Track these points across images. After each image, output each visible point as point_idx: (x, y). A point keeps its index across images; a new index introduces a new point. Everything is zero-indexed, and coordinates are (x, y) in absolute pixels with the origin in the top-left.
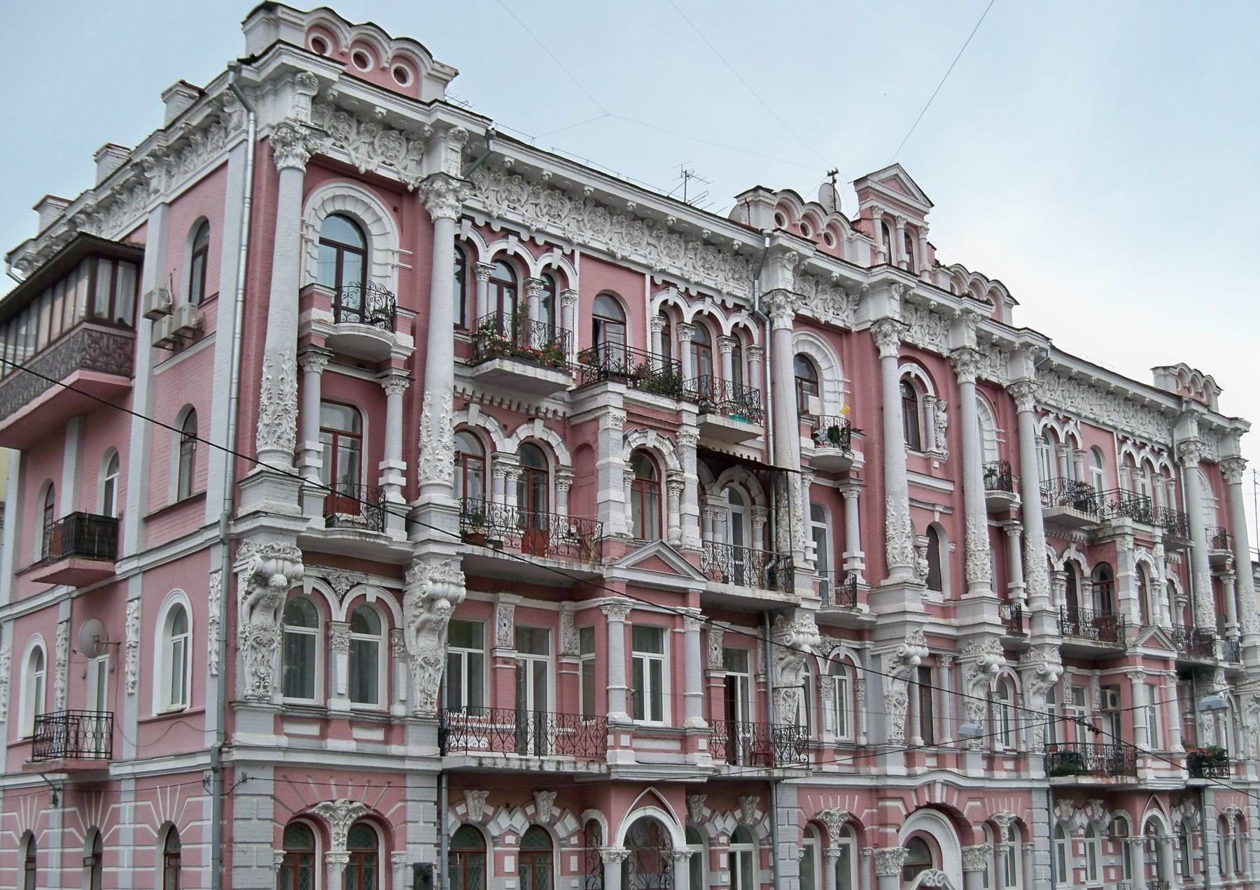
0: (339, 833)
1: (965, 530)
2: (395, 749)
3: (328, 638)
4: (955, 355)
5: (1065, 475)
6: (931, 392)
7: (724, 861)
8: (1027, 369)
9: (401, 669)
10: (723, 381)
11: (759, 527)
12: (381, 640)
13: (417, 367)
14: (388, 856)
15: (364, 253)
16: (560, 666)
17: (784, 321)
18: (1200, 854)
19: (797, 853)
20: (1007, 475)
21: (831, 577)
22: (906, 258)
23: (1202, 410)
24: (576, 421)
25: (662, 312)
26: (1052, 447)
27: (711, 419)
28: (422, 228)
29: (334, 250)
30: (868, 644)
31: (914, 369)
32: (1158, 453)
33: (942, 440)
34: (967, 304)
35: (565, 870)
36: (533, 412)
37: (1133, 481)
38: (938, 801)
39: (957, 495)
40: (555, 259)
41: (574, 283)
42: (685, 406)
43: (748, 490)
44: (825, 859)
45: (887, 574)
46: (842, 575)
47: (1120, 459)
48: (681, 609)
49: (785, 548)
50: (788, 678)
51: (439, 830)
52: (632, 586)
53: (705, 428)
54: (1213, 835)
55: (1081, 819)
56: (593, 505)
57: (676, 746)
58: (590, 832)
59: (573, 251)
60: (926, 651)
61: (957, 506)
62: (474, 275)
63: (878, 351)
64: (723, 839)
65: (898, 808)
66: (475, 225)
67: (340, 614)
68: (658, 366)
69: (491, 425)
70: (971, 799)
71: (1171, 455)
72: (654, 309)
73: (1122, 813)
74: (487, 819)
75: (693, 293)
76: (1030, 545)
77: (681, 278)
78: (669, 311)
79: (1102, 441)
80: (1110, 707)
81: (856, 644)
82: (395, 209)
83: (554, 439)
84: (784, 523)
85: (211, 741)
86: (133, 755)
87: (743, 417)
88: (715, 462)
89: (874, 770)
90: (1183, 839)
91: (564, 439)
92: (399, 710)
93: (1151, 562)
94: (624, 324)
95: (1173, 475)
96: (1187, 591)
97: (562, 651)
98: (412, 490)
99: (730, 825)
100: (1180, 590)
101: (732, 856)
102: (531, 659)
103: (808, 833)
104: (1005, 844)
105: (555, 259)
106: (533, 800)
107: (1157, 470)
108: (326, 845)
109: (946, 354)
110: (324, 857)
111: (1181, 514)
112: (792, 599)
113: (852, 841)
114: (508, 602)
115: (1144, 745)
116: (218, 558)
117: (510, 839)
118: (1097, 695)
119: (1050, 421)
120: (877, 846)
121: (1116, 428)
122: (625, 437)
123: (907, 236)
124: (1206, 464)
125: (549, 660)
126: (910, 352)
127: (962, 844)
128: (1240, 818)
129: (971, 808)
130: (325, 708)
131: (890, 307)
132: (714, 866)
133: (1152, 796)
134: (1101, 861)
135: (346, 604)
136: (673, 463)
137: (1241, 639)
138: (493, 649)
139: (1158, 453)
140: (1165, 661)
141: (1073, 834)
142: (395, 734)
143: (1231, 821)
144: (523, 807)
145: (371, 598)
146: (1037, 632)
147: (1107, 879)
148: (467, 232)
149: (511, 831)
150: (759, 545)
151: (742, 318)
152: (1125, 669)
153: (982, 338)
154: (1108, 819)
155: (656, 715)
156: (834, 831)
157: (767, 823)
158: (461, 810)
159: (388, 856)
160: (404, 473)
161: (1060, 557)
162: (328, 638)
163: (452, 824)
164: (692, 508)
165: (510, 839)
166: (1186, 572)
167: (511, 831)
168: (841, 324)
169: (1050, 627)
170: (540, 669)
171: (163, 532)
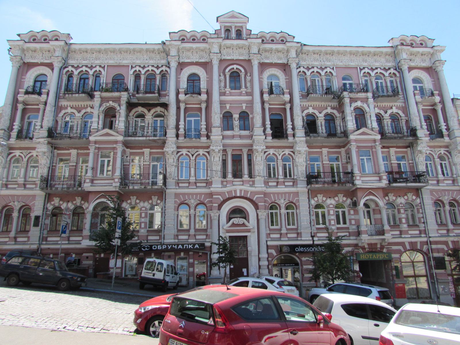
18: (421, 215)
31: (235, 67)
34: (249, 40)
36: (86, 106)
38: (238, 195)
48: (115, 146)
52: (96, 142)
55: (331, 202)
59: (105, 66)
65: (219, 198)
69: (75, 111)
70: (256, 195)
71: (396, 69)
72: (131, 72)
73: (355, 199)
74: (61, 205)
77: (141, 63)
80: (348, 160)
94: (124, 79)
95: (398, 75)
96: (406, 116)
106: (75, 200)
109: (249, 58)
121: (358, 65)
129: (257, 198)
136: (118, 108)
140: (375, 141)
147: (351, 224)
154: (349, 201)
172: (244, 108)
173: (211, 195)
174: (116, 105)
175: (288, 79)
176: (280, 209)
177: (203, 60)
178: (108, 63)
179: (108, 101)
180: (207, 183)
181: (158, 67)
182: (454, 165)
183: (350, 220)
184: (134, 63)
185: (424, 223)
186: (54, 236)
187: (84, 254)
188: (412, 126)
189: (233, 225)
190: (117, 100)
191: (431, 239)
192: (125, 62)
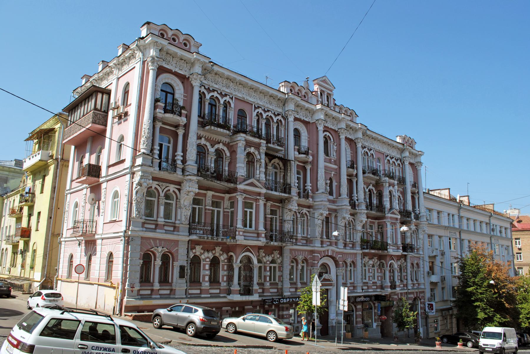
0: (159, 256)
1: (340, 179)
2: (175, 233)
3: (158, 201)
4: (339, 130)
5: (370, 165)
6: (332, 140)
7: (268, 269)
8: (360, 135)
9: (179, 211)
10: (273, 135)
11: (282, 176)
12: (174, 202)
13: (187, 127)
14: (173, 264)
15: (173, 94)
16: (224, 212)
17: (291, 119)
18: (405, 274)
19: (290, 267)
20: (353, 165)
21: (302, 191)
22: (327, 102)
23: (411, 148)
24: (231, 144)
25: (257, 115)
26: (366, 157)
27: (269, 145)
28: (190, 88)
29: (164, 93)
30: (311, 210)
31: (328, 134)
32: (397, 160)
33: (335, 154)
35: (223, 270)
37: (389, 168)
39: (338, 170)
40: (227, 98)
41: (232, 105)
42: (262, 141)
43: (279, 165)
44: (297, 269)
45: (317, 190)
46: (305, 190)
47: (386, 161)
48: (258, 197)
49: (289, 181)
50: (288, 216)
51: (188, 257)
53: (268, 148)
54: (409, 269)
55: (371, 262)
56: (235, 167)
57: (256, 235)
58: (230, 259)
60: (328, 212)
61: (338, 172)
62: (204, 102)
63: (317, 128)
64: (268, 263)
66: (205, 88)
67: (162, 194)
68: (255, 130)
69: (208, 144)
71: (401, 161)
72: (255, 114)
73: (383, 261)
75: (266, 110)
76: (359, 184)
78: (259, 115)
79: (381, 156)
81: (308, 210)
82: (183, 83)
83: (225, 149)
84: (289, 174)
85: (124, 229)
86: (101, 233)
87: (278, 145)
88: (270, 156)
89: (311, 245)
90: (401, 269)
91: (228, 148)
92: (177, 222)
93: (394, 190)
96: (404, 199)
97: (225, 207)
98: (184, 161)
99: (270, 259)
100: (402, 199)
101: (270, 267)
102: (216, 210)
103: (292, 262)
104: (349, 268)
105: (227, 98)
107: (396, 164)
108: (155, 260)
110: (154, 263)
111: (403, 177)
112: (290, 196)
113: (305, 265)
114: (210, 193)
115: (389, 242)
116: (128, 177)
117: (208, 260)
118: (376, 227)
119: (366, 150)
120: (312, 267)
122: (245, 149)
123: (327, 96)
124: (411, 164)
125: (221, 210)
126: (326, 129)
127: (336, 267)
128: (417, 264)
129: (339, 257)
130: (157, 221)
131: (322, 117)
132: (265, 270)
133: (392, 257)
134: (376, 274)
135: (164, 192)
136: (258, 157)
137: (419, 213)
138: (205, 206)
139: (397, 160)
140: (397, 219)
141: (369, 266)
142: (176, 229)
143: (415, 265)
144: (212, 250)
145: (171, 191)
146: (360, 208)
147: (378, 280)
148: (203, 90)
149: (208, 258)
150: (282, 181)
151: (280, 117)
152: (385, 220)
153: (347, 126)
154: (379, 262)
155: (251, 227)
156: (300, 261)
157: (281, 258)
158: (194, 251)
159: (173, 264)
160: (182, 156)
161: (367, 188)
162: (158, 201)
163: (192, 255)
164: (263, 170)
165: (208, 260)
166: (404, 193)
167: (208, 258)
168: (307, 120)
169: (363, 207)
170: (219, 212)
171: (112, 170)
172: (332, 175)
173: (312, 252)
174: (257, 153)
175: (353, 153)
176: (347, 267)
177: (307, 120)
178: (236, 95)
179: (250, 147)
180: (307, 240)
181: (276, 116)
182: (419, 239)
183: (378, 277)
184: (258, 103)
185: (407, 279)
186: (195, 288)
187: (224, 308)
188: (408, 209)
189: (325, 280)
190: (258, 146)
191: (409, 291)
192: (251, 99)
